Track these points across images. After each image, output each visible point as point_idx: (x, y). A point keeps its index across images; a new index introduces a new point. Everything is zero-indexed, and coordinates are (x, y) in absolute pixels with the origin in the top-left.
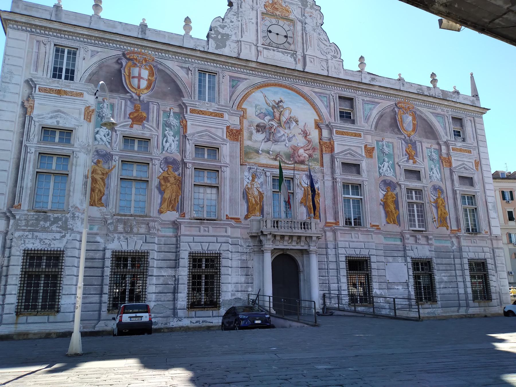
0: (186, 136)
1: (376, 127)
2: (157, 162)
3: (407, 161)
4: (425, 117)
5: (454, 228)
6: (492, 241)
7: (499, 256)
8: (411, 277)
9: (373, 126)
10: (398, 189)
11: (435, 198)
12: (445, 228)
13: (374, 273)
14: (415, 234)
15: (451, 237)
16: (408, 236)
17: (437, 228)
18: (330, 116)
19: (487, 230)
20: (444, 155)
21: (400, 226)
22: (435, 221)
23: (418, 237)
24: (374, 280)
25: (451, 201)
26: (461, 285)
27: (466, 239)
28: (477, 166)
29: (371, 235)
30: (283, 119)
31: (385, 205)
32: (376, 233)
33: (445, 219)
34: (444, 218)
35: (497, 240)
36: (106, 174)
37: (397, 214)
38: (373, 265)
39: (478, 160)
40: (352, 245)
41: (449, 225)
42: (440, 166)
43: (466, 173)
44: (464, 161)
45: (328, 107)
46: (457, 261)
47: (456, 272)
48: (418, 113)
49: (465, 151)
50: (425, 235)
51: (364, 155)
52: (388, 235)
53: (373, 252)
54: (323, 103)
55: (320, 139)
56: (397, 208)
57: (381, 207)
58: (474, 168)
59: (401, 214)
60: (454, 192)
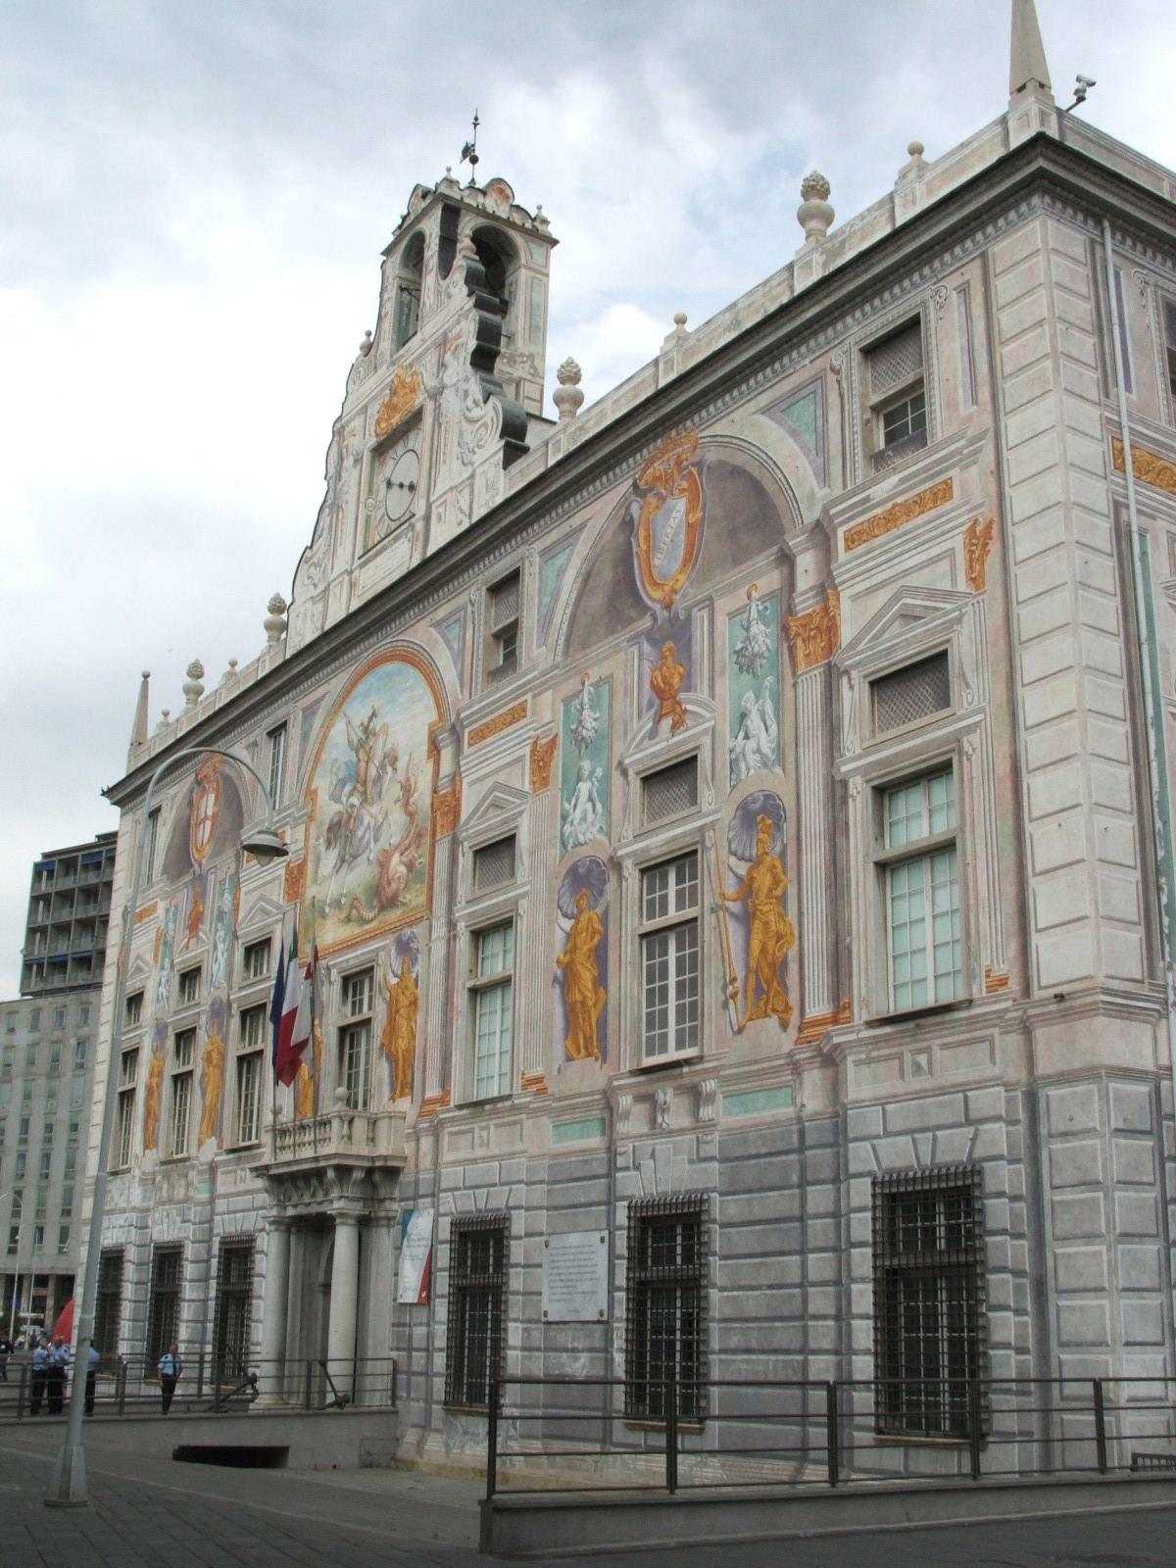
0: (236, 937)
1: (568, 641)
2: (203, 1019)
3: (653, 734)
4: (739, 459)
5: (818, 1007)
6: (1027, 1031)
7: (1066, 1135)
8: (621, 1296)
9: (561, 642)
10: (610, 888)
11: (742, 869)
12: (773, 1022)
13: (516, 1281)
14: (648, 1089)
15: (796, 1068)
16: (625, 1101)
17: (740, 1030)
18: (462, 687)
19: (1007, 967)
20: (805, 603)
21: (604, 1060)
22: (734, 996)
23: (661, 1097)
24: (512, 1314)
25: (814, 859)
26: (823, 1333)
27: (870, 1061)
28: (976, 561)
29: (520, 1122)
30: (373, 772)
31: (567, 980)
32: (535, 1110)
33: (780, 968)
34: (772, 966)
35: (1065, 1016)
36: (160, 1074)
37: (600, 1006)
38: (517, 1251)
39: (988, 512)
40: (475, 1174)
41: (793, 998)
42: (780, 679)
43: (909, 643)
44: (907, 572)
45: (459, 656)
46: (819, 1197)
47: (804, 1265)
48: (712, 456)
49: (920, 504)
50: (687, 1081)
51: (527, 787)
52: (566, 1112)
53: (521, 1194)
54: (450, 648)
55: (435, 791)
56: (601, 981)
57: (557, 989)
58: (962, 585)
59: (610, 1009)
60: (837, 793)
